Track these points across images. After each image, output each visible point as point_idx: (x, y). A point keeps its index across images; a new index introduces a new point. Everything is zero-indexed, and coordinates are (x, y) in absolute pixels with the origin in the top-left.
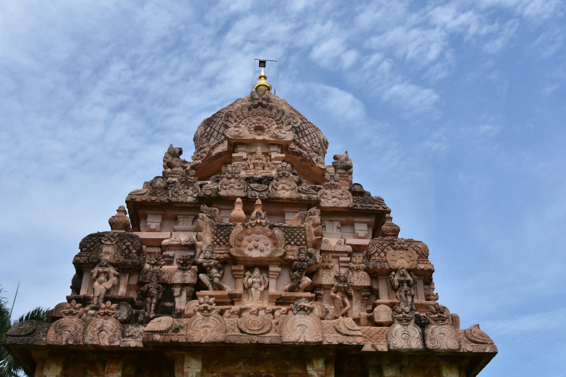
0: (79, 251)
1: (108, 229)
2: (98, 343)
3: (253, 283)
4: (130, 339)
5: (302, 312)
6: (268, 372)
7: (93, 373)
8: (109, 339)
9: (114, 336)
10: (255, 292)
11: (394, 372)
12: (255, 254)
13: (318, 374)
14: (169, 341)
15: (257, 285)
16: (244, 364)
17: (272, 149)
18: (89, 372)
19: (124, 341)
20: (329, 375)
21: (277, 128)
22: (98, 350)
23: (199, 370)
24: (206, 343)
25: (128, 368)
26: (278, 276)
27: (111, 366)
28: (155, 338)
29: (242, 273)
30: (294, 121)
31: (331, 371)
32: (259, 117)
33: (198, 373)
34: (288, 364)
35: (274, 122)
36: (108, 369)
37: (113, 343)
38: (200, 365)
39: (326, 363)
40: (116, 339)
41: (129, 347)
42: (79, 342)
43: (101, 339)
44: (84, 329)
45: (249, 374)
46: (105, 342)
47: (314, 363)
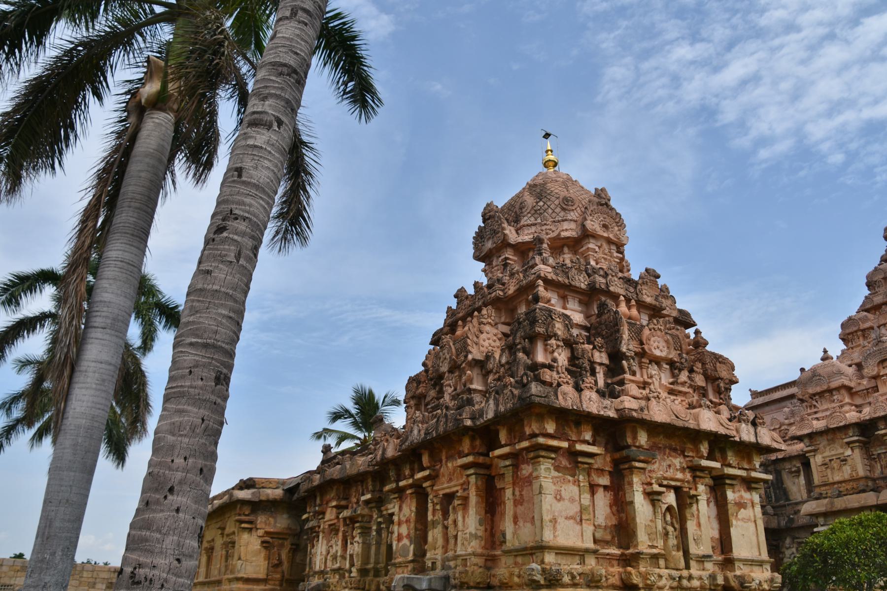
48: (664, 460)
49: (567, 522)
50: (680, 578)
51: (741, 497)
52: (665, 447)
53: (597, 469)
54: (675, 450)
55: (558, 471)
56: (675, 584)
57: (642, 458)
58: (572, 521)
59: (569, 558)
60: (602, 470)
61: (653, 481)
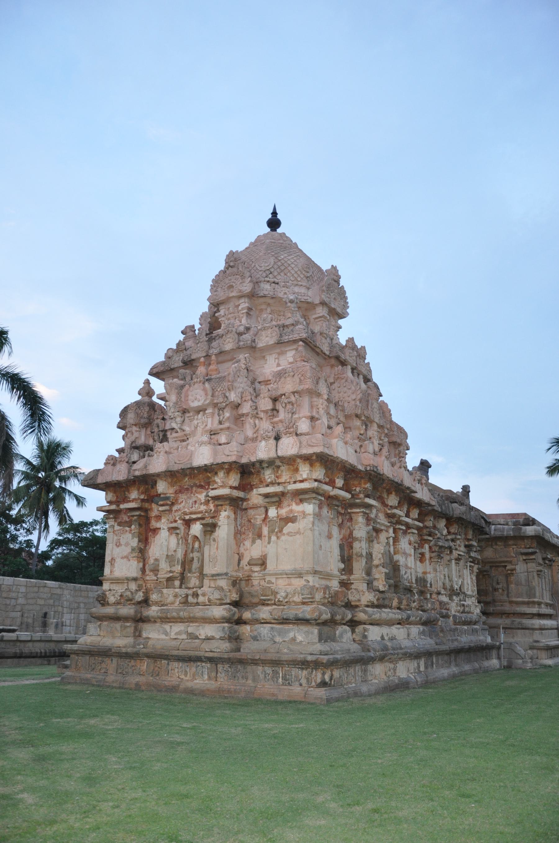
0: (120, 419)
1: (139, 398)
3: (198, 423)
5: (203, 445)
10: (199, 430)
12: (196, 404)
15: (199, 424)
17: (241, 301)
21: (241, 283)
26: (213, 414)
29: (192, 418)
30: (267, 265)
32: (229, 278)
34: (209, 475)
35: (240, 279)
48: (190, 498)
50: (187, 596)
51: (291, 511)
52: (192, 487)
54: (201, 487)
55: (120, 526)
58: (125, 560)
61: (177, 519)
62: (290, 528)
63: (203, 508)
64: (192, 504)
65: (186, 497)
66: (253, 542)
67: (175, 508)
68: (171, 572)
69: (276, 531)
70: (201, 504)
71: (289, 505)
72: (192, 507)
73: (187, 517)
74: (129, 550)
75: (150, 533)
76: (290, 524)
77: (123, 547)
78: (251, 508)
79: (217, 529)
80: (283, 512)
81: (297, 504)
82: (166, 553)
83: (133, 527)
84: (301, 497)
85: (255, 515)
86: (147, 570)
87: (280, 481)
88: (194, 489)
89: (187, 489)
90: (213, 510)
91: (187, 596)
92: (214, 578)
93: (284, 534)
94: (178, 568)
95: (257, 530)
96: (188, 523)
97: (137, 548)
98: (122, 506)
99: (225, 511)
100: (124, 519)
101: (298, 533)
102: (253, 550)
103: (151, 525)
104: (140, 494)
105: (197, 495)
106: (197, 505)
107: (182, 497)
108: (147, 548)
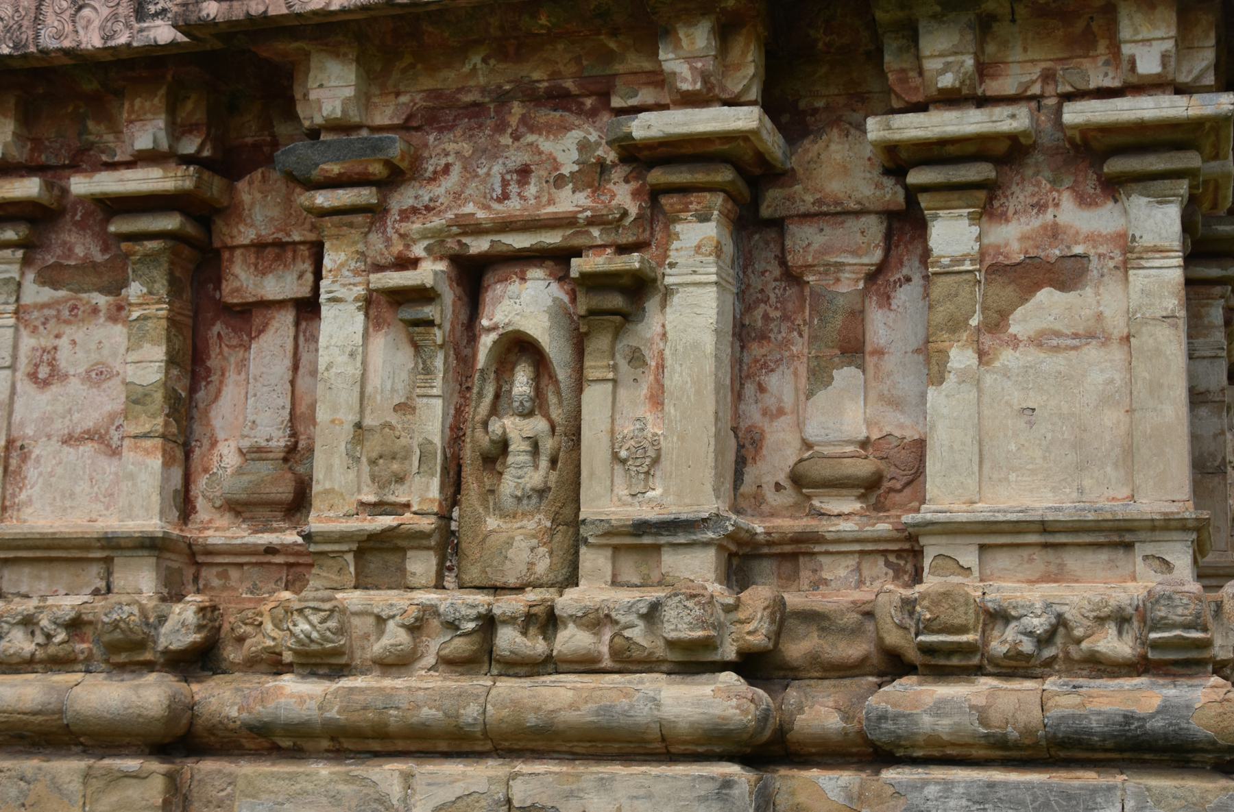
2: (74, 44)
4: (158, 22)
6: (555, 75)
7: (102, 128)
8: (102, 28)
9: (115, 17)
11: (956, 39)
13: (692, 69)
14: (241, 17)
16: (484, 61)
18: (91, 125)
19: (141, 30)
20: (738, 67)
22: (79, 61)
23: (350, 92)
24: (343, 11)
25: (189, 105)
27: (138, 102)
28: (204, 13)
31: (744, 54)
33: (349, 99)
34: (612, 45)
36: (131, 111)
37: (111, 37)
38: (353, 77)
39: (725, 33)
40: (119, 26)
41: (157, 46)
42: (25, 46)
43: (81, 32)
44: (38, 8)
45: (500, 87)
46: (92, 40)
47: (681, 35)
48: (494, 152)
49: (69, 453)
50: (489, 623)
51: (1054, 232)
52: (503, 99)
53: (259, 247)
54: (559, 99)
55: (55, 285)
56: (459, 646)
57: (335, 169)
58: (88, 448)
59: (64, 575)
60: (280, 245)
61: (418, 250)
62: (1047, 307)
63: (569, 201)
64: (505, 184)
65: (466, 148)
66: (819, 376)
67: (404, 198)
68: (379, 508)
69: (974, 322)
70: (560, 181)
71: (1041, 207)
72: (505, 196)
73: (479, 246)
74: (110, 400)
75: (218, 327)
76: (1046, 296)
77: (74, 385)
78: (806, 216)
79: (652, 305)
80: (1012, 235)
81: (1084, 201)
82: (353, 418)
83: (135, 290)
84: (1115, 166)
85: (826, 250)
86: (200, 503)
87: (994, 87)
88: (517, 109)
89: (475, 110)
90: (633, 211)
91: (489, 623)
92: (647, 540)
93: (1015, 342)
94: (423, 492)
95: (838, 321)
96: (473, 276)
97: (159, 396)
98: (80, 185)
99: (704, 218)
100: (80, 251)
101: (1094, 334)
102: (842, 416)
103: (227, 287)
104: (176, 130)
105: (531, 138)
106: (532, 190)
107: (448, 148)
108: (201, 395)
